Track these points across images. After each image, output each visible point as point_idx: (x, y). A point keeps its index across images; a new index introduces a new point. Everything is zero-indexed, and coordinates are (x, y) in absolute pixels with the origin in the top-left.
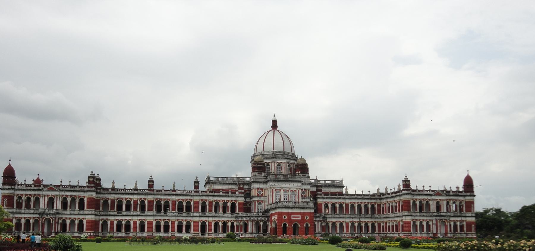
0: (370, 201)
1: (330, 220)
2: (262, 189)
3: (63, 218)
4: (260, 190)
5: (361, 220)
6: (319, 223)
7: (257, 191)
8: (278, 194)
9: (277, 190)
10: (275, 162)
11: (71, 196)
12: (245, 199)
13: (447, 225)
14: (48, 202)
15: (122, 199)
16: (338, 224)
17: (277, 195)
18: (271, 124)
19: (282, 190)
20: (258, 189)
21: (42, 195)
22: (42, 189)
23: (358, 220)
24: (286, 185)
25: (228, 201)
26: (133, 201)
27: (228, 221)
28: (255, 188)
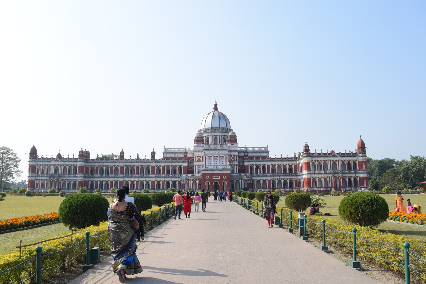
0: (287, 163)
1: (255, 178)
2: (200, 156)
3: (64, 180)
4: (199, 157)
5: (281, 178)
6: (243, 181)
8: (215, 160)
11: (69, 165)
12: (189, 163)
13: (341, 181)
14: (63, 169)
15: (103, 166)
16: (261, 182)
17: (209, 161)
19: (213, 157)
20: (197, 156)
21: (52, 165)
22: (51, 161)
23: (278, 178)
25: (176, 165)
26: (110, 167)
27: (176, 180)
28: (195, 155)
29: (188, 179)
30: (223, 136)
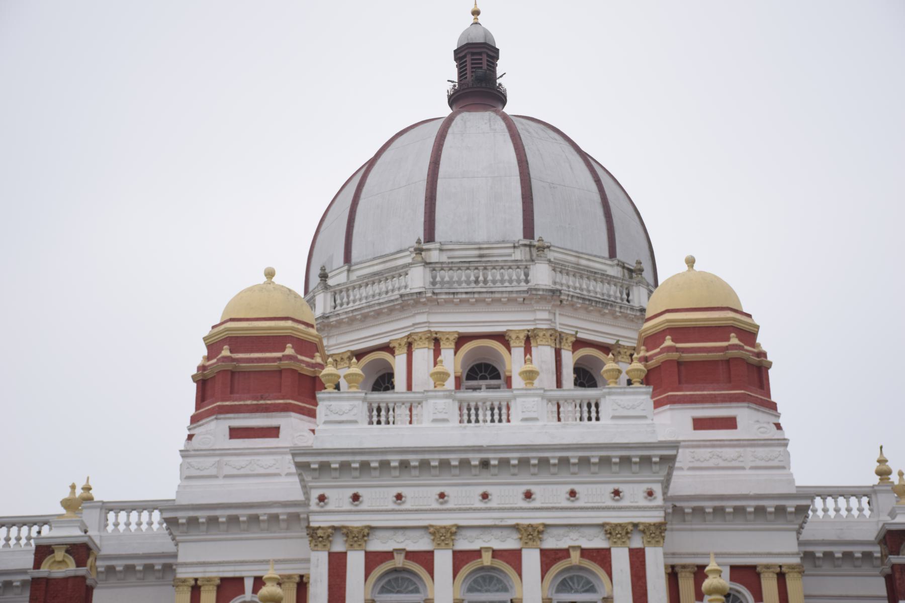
9: (388, 555)
10: (437, 342)
24: (485, 496)
28: (198, 573)
30: (579, 344)
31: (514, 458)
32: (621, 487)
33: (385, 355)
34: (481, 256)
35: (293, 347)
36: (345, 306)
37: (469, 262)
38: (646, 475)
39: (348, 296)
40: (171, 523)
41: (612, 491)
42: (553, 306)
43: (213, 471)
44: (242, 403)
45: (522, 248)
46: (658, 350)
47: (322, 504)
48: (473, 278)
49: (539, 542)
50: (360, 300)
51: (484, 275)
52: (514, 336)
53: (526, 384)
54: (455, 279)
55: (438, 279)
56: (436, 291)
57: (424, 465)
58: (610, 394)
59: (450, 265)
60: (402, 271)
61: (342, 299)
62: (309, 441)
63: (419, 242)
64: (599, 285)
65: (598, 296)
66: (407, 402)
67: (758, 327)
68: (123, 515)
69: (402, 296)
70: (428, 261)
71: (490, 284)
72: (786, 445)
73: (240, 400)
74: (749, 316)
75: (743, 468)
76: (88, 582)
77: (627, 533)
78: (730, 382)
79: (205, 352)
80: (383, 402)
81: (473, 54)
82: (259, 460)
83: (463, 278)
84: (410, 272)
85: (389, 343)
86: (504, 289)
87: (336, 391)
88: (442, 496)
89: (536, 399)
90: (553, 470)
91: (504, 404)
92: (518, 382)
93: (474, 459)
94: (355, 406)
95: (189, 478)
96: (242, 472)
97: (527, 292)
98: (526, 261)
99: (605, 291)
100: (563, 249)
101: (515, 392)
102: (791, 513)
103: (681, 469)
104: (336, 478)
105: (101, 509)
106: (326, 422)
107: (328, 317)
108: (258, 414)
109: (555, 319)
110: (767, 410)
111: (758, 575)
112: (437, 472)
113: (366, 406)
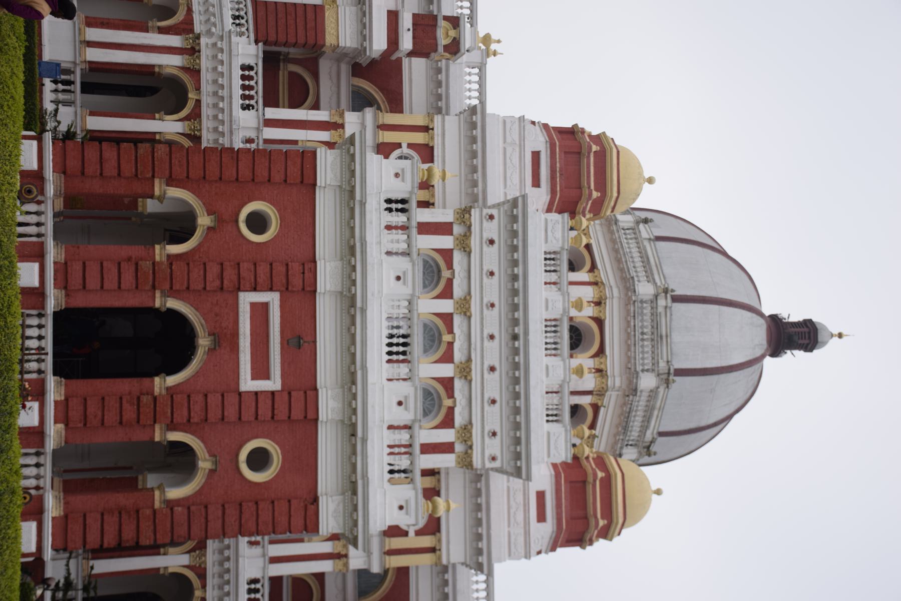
7: (410, 146)
9: (450, 266)
18: (794, 314)
24: (492, 337)
28: (437, 131)
29: (192, 31)
30: (596, 408)
31: (519, 359)
32: (498, 437)
33: (588, 266)
34: (661, 337)
35: (597, 197)
36: (624, 236)
37: (657, 328)
38: (507, 456)
39: (631, 239)
40: (473, 110)
41: (496, 431)
42: (625, 390)
43: (509, 140)
44: (558, 160)
45: (667, 368)
46: (594, 466)
47: (488, 217)
48: (645, 330)
49: (458, 376)
50: (629, 248)
51: (647, 339)
52: (602, 360)
53: (573, 369)
54: (645, 318)
55: (645, 305)
56: (636, 304)
57: (515, 292)
58: (566, 431)
59: (655, 314)
60: (650, 278)
61: (629, 234)
62: (531, 209)
63: (673, 291)
64: (639, 424)
65: (631, 423)
66: (561, 281)
67: (611, 540)
68: (476, 78)
69: (633, 278)
70: (659, 298)
71: (641, 343)
72: (526, 557)
73: (560, 159)
74: (619, 534)
75: (509, 526)
76: (433, 54)
77: (465, 441)
78: (571, 519)
79: (594, 133)
80: (560, 263)
81: (809, 333)
82: (516, 172)
83: (645, 324)
84: (650, 284)
85: (597, 269)
86: (637, 354)
87: (569, 228)
88: (493, 305)
89: (562, 376)
90: (511, 388)
91: (558, 352)
92: (575, 362)
93: (519, 329)
94: (558, 241)
95: (504, 122)
96: (508, 161)
97: (635, 370)
98: (658, 371)
99: (634, 428)
100: (666, 397)
101: (567, 361)
102: (478, 559)
103: (508, 481)
104: (506, 228)
105: (481, 63)
106: (546, 220)
107: (616, 224)
108: (549, 171)
109: (615, 391)
110: (550, 545)
111: (433, 534)
112: (510, 301)
113: (557, 249)
